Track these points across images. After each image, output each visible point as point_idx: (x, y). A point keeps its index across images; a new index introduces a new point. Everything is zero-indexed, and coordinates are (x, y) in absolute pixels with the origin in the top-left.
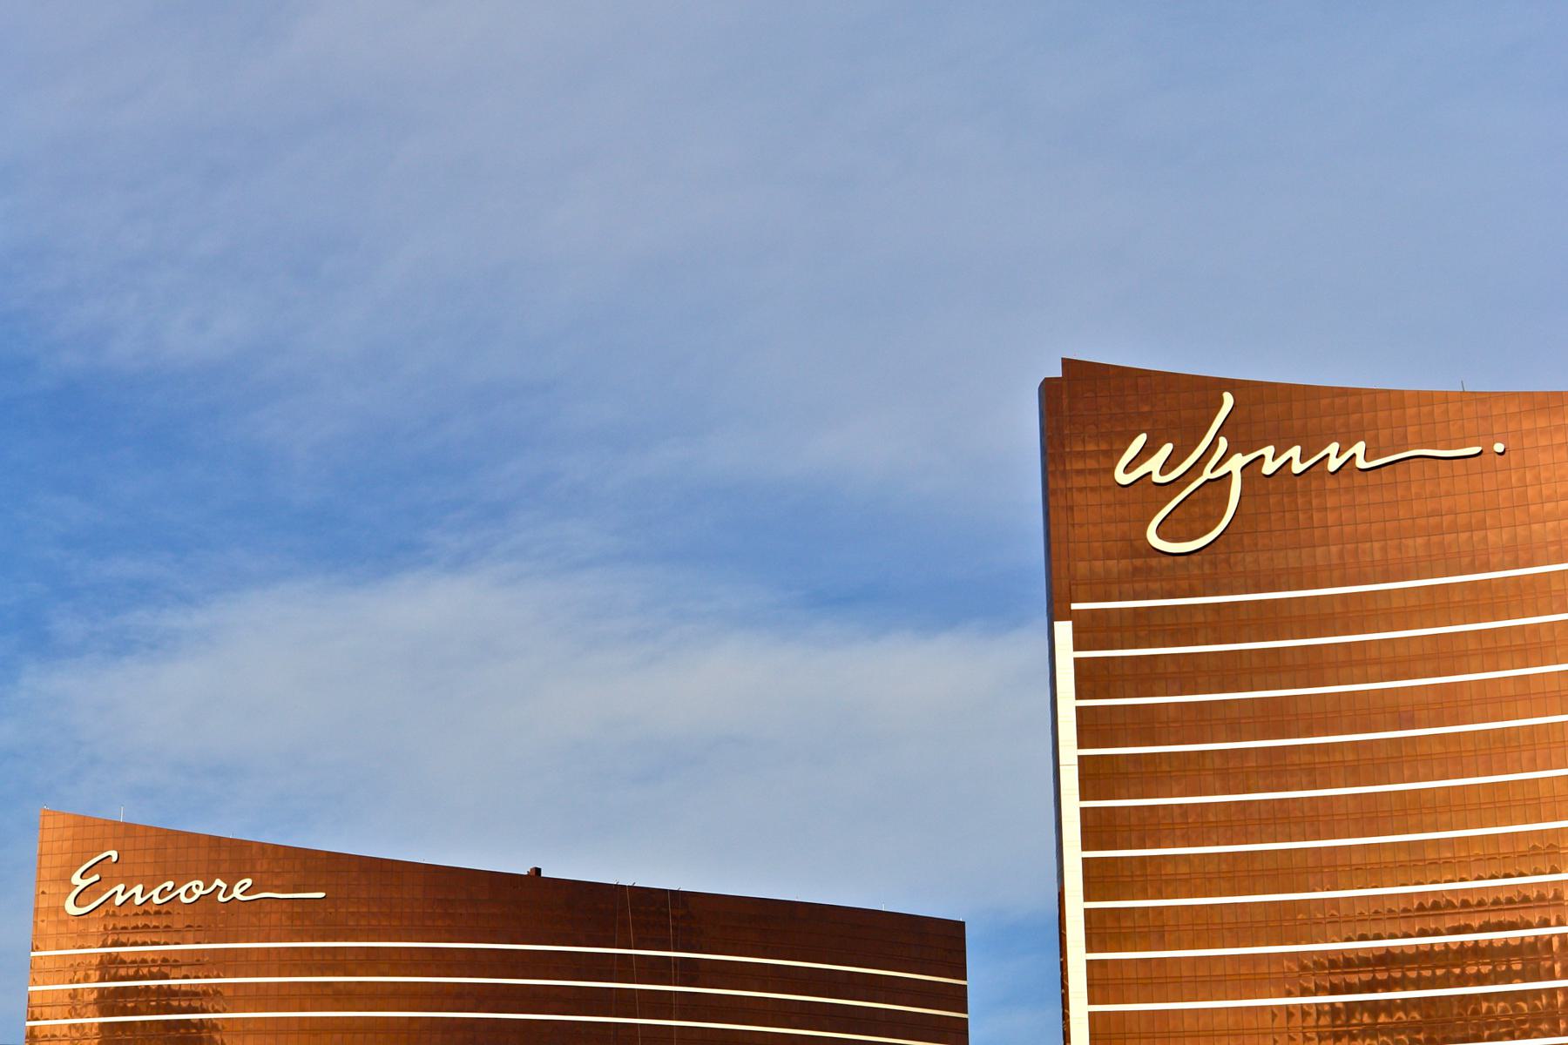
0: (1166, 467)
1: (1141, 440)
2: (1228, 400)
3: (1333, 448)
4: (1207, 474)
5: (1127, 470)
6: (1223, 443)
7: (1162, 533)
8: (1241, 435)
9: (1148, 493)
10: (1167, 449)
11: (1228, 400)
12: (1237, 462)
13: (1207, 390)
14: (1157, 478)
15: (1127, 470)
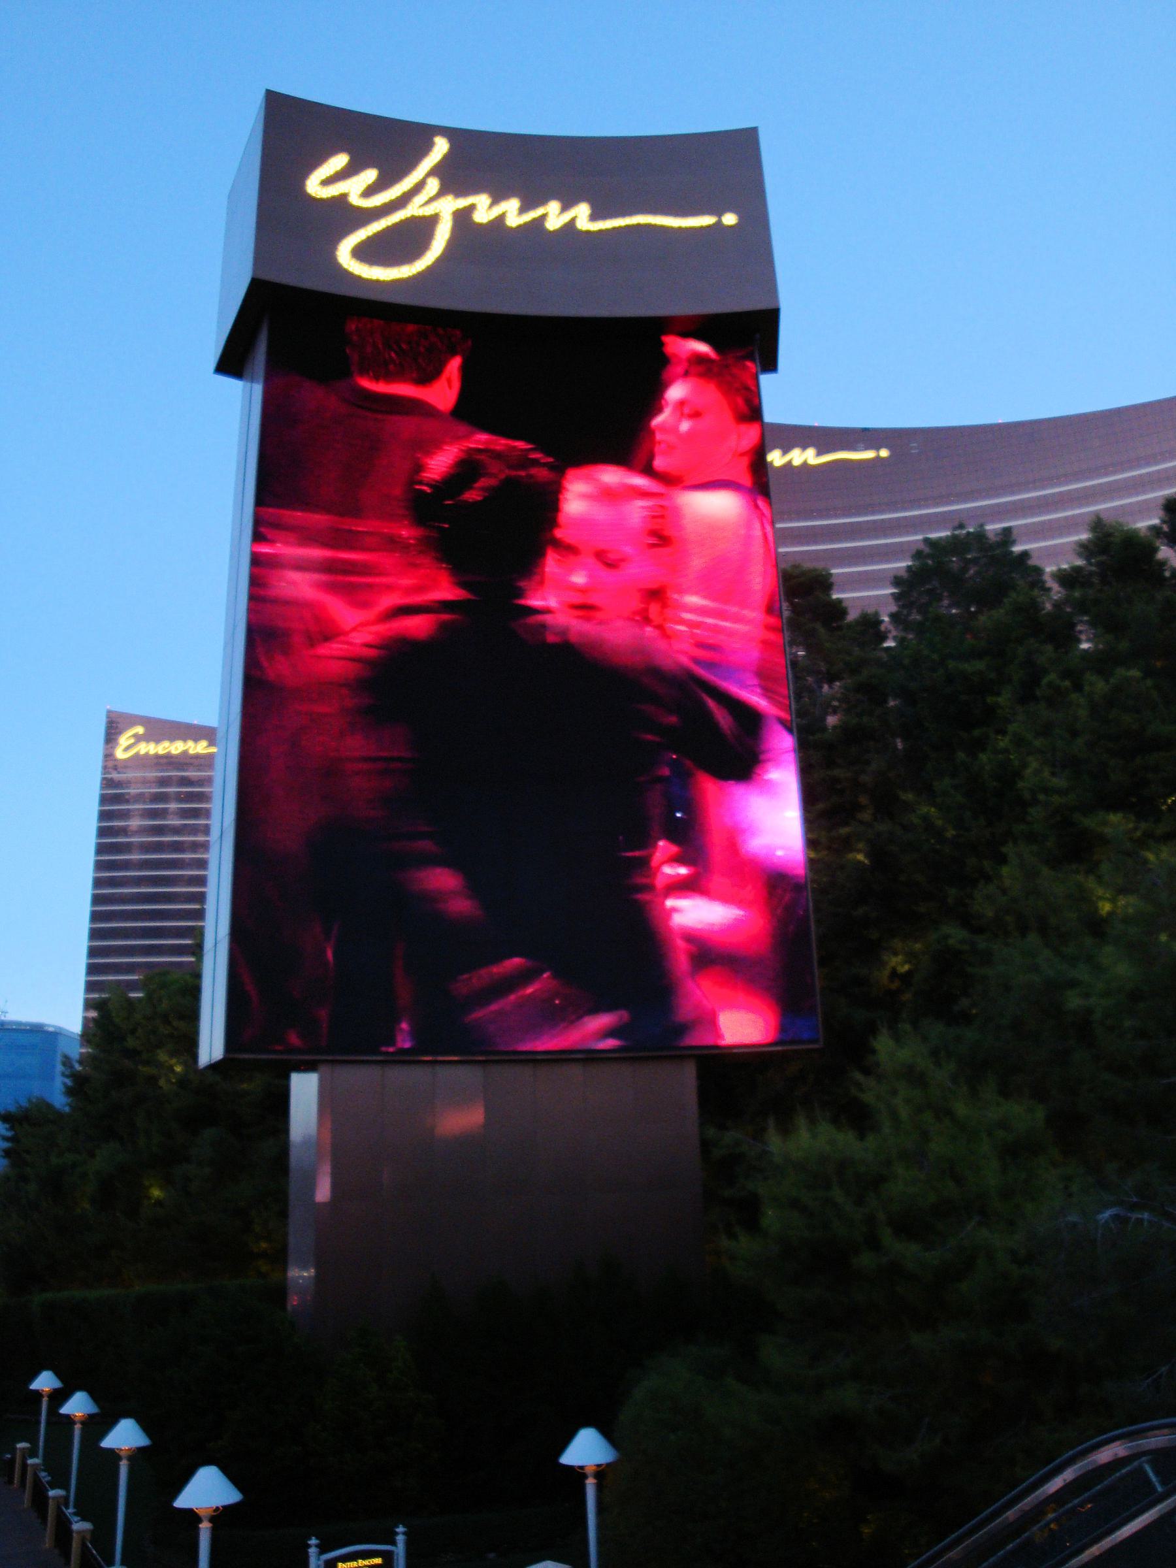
0: (369, 192)
1: (340, 161)
2: (441, 146)
3: (553, 207)
4: (414, 209)
5: (327, 182)
6: (433, 185)
7: (360, 253)
8: (453, 178)
9: (343, 216)
10: (370, 176)
11: (441, 146)
12: (448, 206)
13: (415, 138)
14: (356, 200)
15: (327, 182)
